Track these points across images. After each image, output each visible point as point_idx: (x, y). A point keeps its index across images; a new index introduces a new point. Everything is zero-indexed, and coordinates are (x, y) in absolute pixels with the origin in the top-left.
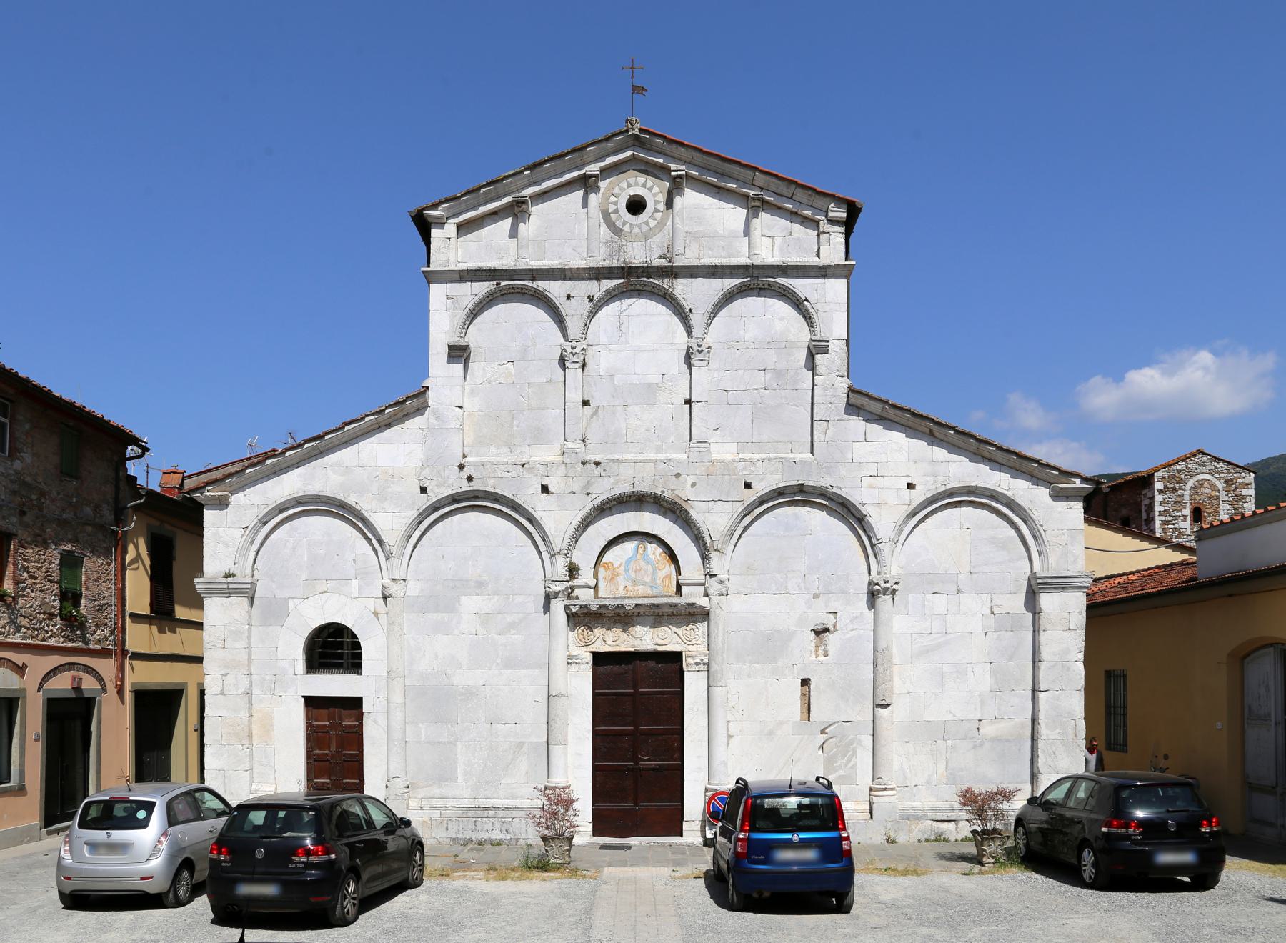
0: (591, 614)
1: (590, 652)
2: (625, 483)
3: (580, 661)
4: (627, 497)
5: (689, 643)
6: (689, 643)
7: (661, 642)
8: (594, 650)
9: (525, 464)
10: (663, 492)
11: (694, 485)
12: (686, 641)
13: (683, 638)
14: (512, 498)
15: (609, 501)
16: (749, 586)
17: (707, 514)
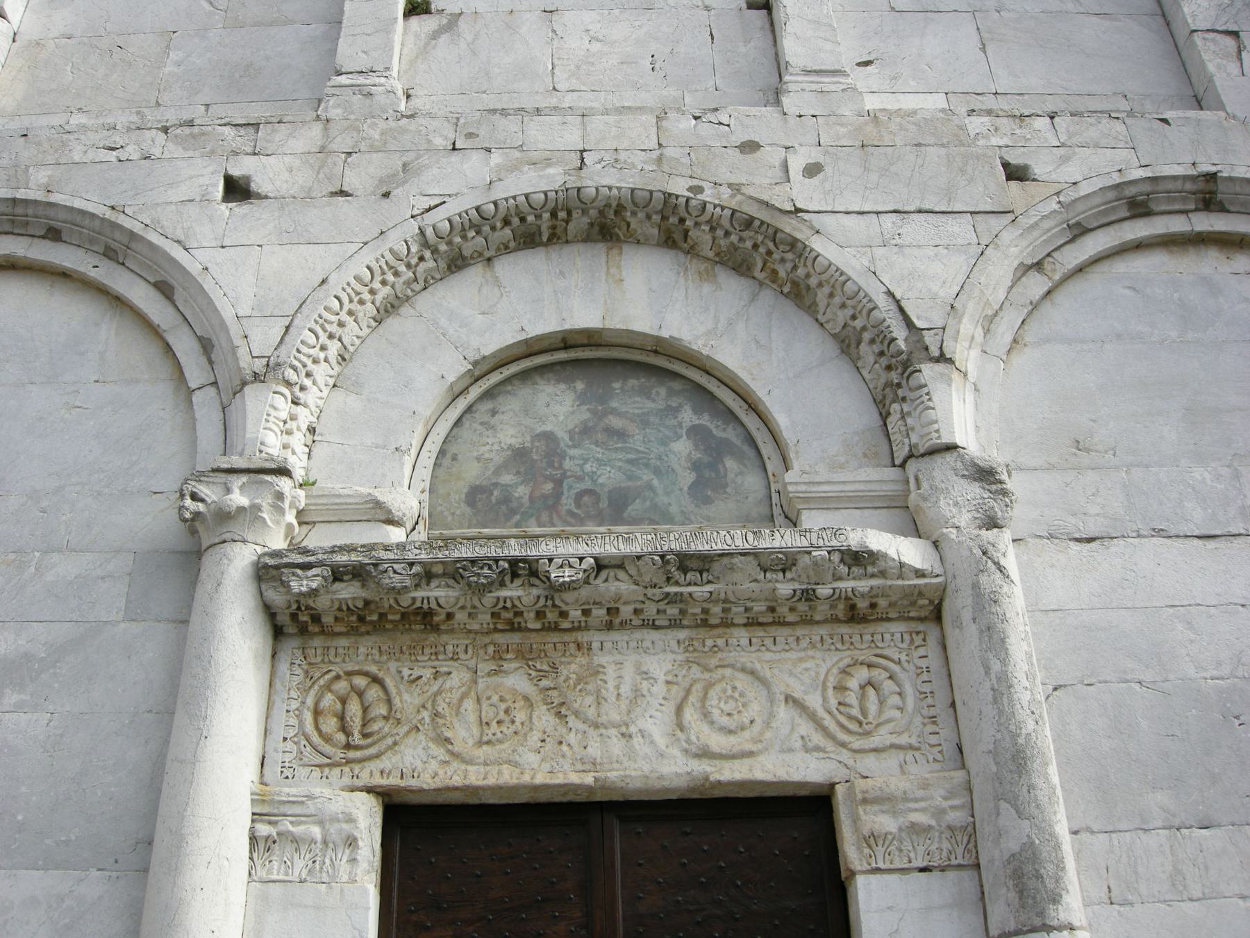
0: (382, 616)
1: (369, 790)
2: (549, 165)
3: (316, 831)
4: (554, 215)
5: (856, 745)
6: (857, 744)
7: (717, 742)
8: (393, 781)
9: (157, 102)
10: (698, 190)
11: (812, 170)
12: (843, 736)
13: (829, 722)
14: (109, 214)
15: (478, 222)
16: (1094, 510)
17: (880, 252)
